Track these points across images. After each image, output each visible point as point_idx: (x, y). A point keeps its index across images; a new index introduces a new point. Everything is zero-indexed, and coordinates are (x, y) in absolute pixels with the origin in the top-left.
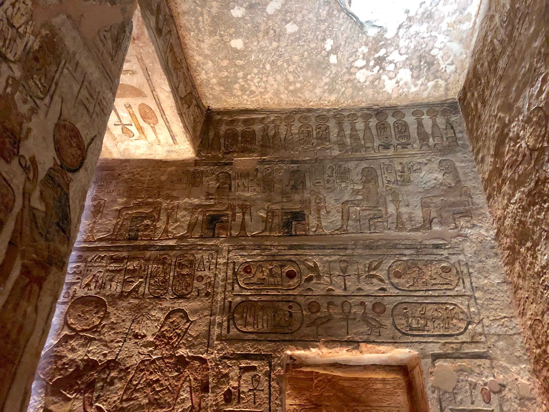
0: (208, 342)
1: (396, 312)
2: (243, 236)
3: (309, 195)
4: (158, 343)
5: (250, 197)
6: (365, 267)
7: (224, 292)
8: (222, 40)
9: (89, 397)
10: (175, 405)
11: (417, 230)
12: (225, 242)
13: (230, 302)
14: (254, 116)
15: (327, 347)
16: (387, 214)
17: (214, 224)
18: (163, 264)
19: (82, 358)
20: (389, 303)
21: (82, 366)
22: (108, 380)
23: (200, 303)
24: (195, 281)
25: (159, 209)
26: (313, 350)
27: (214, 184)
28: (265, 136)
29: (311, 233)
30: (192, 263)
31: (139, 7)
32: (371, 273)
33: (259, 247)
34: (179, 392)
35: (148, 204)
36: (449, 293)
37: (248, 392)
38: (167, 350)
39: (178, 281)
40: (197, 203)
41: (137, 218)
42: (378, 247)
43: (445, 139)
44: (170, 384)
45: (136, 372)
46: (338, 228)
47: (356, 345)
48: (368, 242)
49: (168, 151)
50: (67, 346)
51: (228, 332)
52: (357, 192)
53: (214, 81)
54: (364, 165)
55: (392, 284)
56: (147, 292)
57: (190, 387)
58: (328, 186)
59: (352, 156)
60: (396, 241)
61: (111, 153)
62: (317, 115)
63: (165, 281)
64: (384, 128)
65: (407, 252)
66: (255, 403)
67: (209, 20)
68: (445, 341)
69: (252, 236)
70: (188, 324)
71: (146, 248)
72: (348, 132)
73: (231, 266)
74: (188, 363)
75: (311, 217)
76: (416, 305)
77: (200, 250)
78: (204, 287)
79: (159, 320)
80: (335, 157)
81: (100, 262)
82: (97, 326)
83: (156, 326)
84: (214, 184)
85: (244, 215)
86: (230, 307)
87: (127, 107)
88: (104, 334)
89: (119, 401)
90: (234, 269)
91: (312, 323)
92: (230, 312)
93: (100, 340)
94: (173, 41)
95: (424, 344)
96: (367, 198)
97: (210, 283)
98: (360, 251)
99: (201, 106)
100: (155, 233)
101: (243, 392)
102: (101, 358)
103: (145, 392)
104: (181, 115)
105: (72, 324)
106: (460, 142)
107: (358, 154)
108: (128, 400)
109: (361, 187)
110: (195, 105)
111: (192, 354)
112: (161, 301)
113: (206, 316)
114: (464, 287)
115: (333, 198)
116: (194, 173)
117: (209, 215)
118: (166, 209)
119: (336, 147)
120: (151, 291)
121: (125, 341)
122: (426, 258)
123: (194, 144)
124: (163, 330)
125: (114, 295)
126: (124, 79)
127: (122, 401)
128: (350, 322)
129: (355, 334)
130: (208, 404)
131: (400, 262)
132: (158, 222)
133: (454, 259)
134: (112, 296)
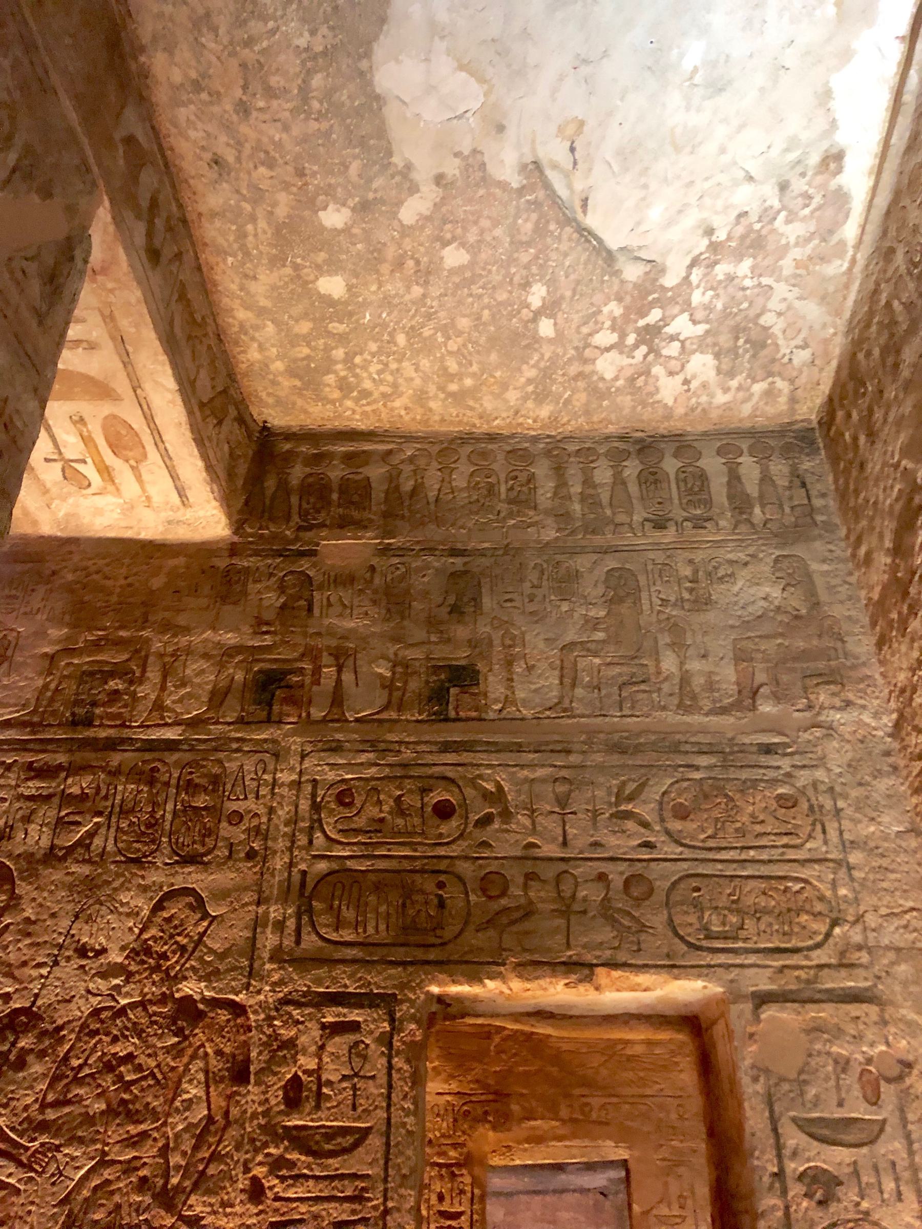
0: (251, 966)
1: (676, 897)
2: (338, 721)
3: (488, 629)
4: (133, 968)
5: (351, 630)
6: (609, 794)
7: (290, 849)
8: (299, 277)
10: (168, 1115)
11: (724, 711)
12: (294, 733)
13: (304, 873)
14: (368, 447)
15: (520, 976)
16: (659, 673)
17: (271, 690)
18: (151, 783)
20: (663, 877)
22: (12, 1057)
23: (233, 875)
24: (224, 824)
26: (490, 984)
27: (273, 599)
28: (393, 490)
29: (491, 715)
30: (216, 781)
31: (107, 203)
32: (623, 808)
33: (373, 745)
34: (179, 1082)
35: (120, 643)
36: (791, 854)
37: (340, 1081)
38: (154, 983)
39: (185, 823)
40: (232, 642)
41: (92, 674)
42: (638, 749)
43: (787, 510)
44: (158, 1066)
45: (78, 1039)
46: (550, 704)
47: (586, 971)
48: (616, 737)
49: (169, 522)
51: (298, 942)
52: (594, 624)
53: (279, 366)
54: (611, 563)
55: (668, 832)
56: (110, 847)
57: (207, 1072)
58: (531, 608)
59: (583, 543)
60: (678, 737)
61: (35, 523)
62: (509, 448)
64: (656, 482)
65: (703, 761)
66: (354, 1108)
67: (269, 232)
68: (781, 963)
69: (357, 720)
70: (205, 924)
71: (111, 745)
72: (576, 489)
73: (309, 788)
74: (201, 1015)
75: (491, 678)
76: (721, 881)
77: (237, 750)
78: (243, 837)
79: (138, 914)
80: (548, 543)
83: (130, 929)
84: (273, 599)
85: (339, 671)
86: (303, 884)
87: (75, 423)
90: (314, 795)
91: (488, 922)
92: (301, 894)
94: (186, 275)
95: (737, 971)
96: (615, 639)
97: (257, 829)
98: (599, 758)
100: (133, 709)
101: (329, 1083)
103: (99, 1085)
104: (200, 441)
106: (819, 518)
107: (598, 540)
108: (56, 1104)
109: (602, 613)
110: (235, 419)
111: (212, 994)
112: (144, 868)
113: (247, 904)
114: (826, 842)
115: (542, 636)
116: (227, 572)
117: (260, 671)
118: (161, 656)
119: (550, 521)
120: (120, 845)
122: (744, 775)
123: (229, 506)
124: (145, 936)
125: (32, 854)
126: (70, 360)
127: (44, 1106)
128: (573, 918)
129: (584, 946)
130: (245, 1111)
131: (685, 784)
132: (141, 684)
133: (803, 778)
134: (29, 857)
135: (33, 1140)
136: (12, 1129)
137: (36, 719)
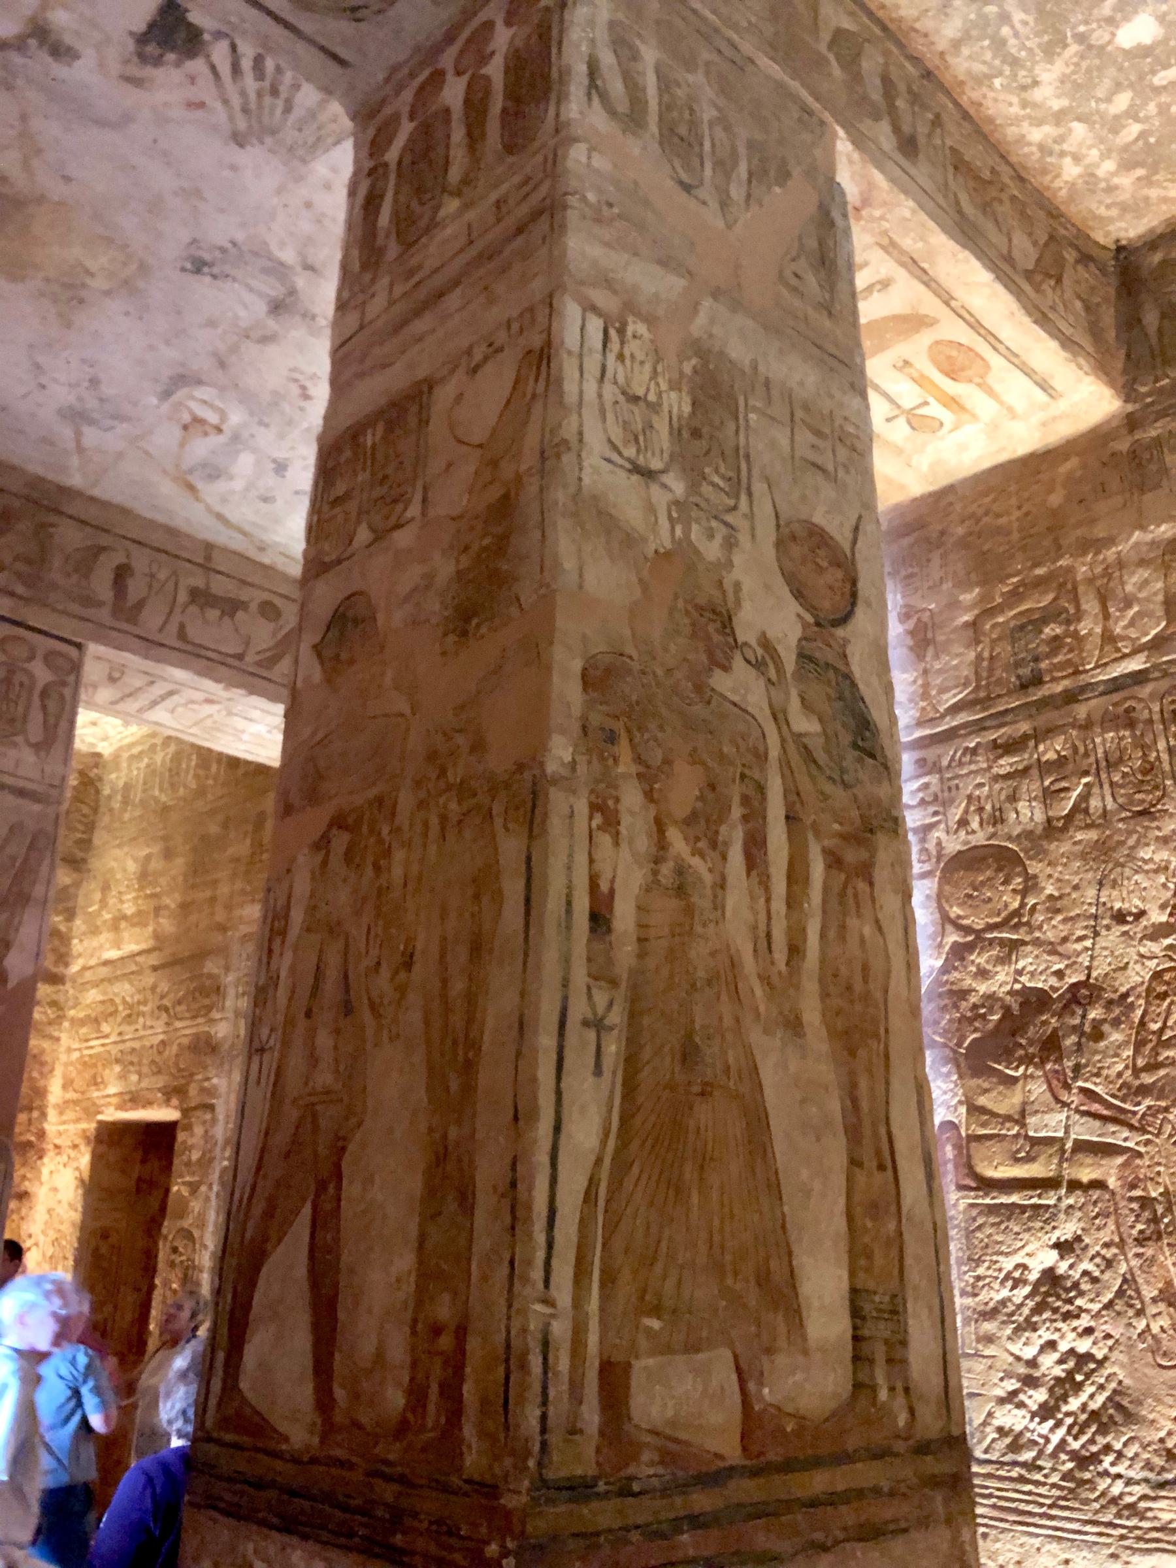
8: (1090, 47)
9: (1057, 1072)
18: (1131, 724)
19: (1008, 988)
21: (1016, 1008)
25: (1069, 586)
31: (841, 132)
35: (1040, 583)
41: (1022, 628)
45: (1148, 1003)
50: (965, 967)
53: (1109, 166)
56: (1110, 804)
61: (902, 487)
63: (1149, 768)
67: (1031, 19)
71: (1071, 697)
79: (1166, 868)
81: (971, 762)
82: (1017, 913)
83: (1164, 885)
87: (900, 369)
88: (1040, 927)
89: (1129, 1072)
93: (1037, 942)
94: (954, 135)
99: (1095, 252)
100: (1082, 651)
102: (1053, 981)
104: (1042, 319)
105: (959, 917)
110: (1077, 262)
112: (1155, 819)
118: (1090, 581)
120: (1120, 800)
121: (1096, 934)
123: (1107, 374)
125: (1031, 832)
126: (869, 310)
132: (1079, 620)
134: (1028, 834)
135: (1138, 1104)
136: (1113, 1096)
137: (982, 694)
